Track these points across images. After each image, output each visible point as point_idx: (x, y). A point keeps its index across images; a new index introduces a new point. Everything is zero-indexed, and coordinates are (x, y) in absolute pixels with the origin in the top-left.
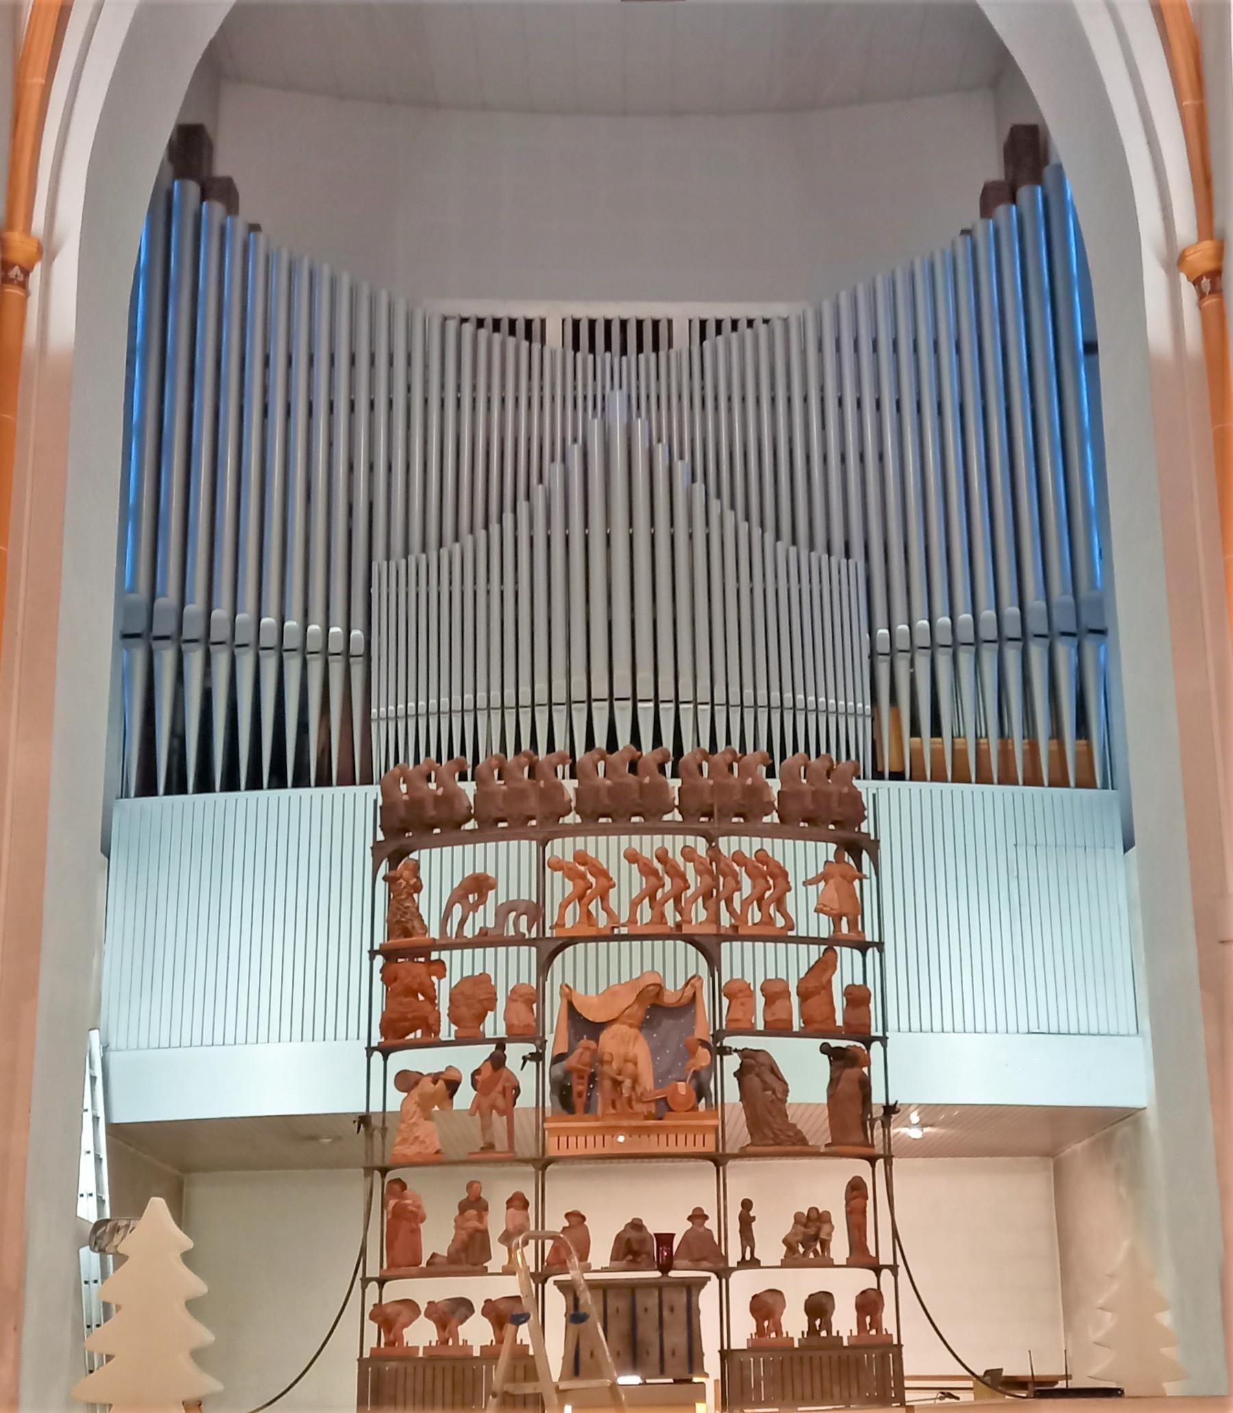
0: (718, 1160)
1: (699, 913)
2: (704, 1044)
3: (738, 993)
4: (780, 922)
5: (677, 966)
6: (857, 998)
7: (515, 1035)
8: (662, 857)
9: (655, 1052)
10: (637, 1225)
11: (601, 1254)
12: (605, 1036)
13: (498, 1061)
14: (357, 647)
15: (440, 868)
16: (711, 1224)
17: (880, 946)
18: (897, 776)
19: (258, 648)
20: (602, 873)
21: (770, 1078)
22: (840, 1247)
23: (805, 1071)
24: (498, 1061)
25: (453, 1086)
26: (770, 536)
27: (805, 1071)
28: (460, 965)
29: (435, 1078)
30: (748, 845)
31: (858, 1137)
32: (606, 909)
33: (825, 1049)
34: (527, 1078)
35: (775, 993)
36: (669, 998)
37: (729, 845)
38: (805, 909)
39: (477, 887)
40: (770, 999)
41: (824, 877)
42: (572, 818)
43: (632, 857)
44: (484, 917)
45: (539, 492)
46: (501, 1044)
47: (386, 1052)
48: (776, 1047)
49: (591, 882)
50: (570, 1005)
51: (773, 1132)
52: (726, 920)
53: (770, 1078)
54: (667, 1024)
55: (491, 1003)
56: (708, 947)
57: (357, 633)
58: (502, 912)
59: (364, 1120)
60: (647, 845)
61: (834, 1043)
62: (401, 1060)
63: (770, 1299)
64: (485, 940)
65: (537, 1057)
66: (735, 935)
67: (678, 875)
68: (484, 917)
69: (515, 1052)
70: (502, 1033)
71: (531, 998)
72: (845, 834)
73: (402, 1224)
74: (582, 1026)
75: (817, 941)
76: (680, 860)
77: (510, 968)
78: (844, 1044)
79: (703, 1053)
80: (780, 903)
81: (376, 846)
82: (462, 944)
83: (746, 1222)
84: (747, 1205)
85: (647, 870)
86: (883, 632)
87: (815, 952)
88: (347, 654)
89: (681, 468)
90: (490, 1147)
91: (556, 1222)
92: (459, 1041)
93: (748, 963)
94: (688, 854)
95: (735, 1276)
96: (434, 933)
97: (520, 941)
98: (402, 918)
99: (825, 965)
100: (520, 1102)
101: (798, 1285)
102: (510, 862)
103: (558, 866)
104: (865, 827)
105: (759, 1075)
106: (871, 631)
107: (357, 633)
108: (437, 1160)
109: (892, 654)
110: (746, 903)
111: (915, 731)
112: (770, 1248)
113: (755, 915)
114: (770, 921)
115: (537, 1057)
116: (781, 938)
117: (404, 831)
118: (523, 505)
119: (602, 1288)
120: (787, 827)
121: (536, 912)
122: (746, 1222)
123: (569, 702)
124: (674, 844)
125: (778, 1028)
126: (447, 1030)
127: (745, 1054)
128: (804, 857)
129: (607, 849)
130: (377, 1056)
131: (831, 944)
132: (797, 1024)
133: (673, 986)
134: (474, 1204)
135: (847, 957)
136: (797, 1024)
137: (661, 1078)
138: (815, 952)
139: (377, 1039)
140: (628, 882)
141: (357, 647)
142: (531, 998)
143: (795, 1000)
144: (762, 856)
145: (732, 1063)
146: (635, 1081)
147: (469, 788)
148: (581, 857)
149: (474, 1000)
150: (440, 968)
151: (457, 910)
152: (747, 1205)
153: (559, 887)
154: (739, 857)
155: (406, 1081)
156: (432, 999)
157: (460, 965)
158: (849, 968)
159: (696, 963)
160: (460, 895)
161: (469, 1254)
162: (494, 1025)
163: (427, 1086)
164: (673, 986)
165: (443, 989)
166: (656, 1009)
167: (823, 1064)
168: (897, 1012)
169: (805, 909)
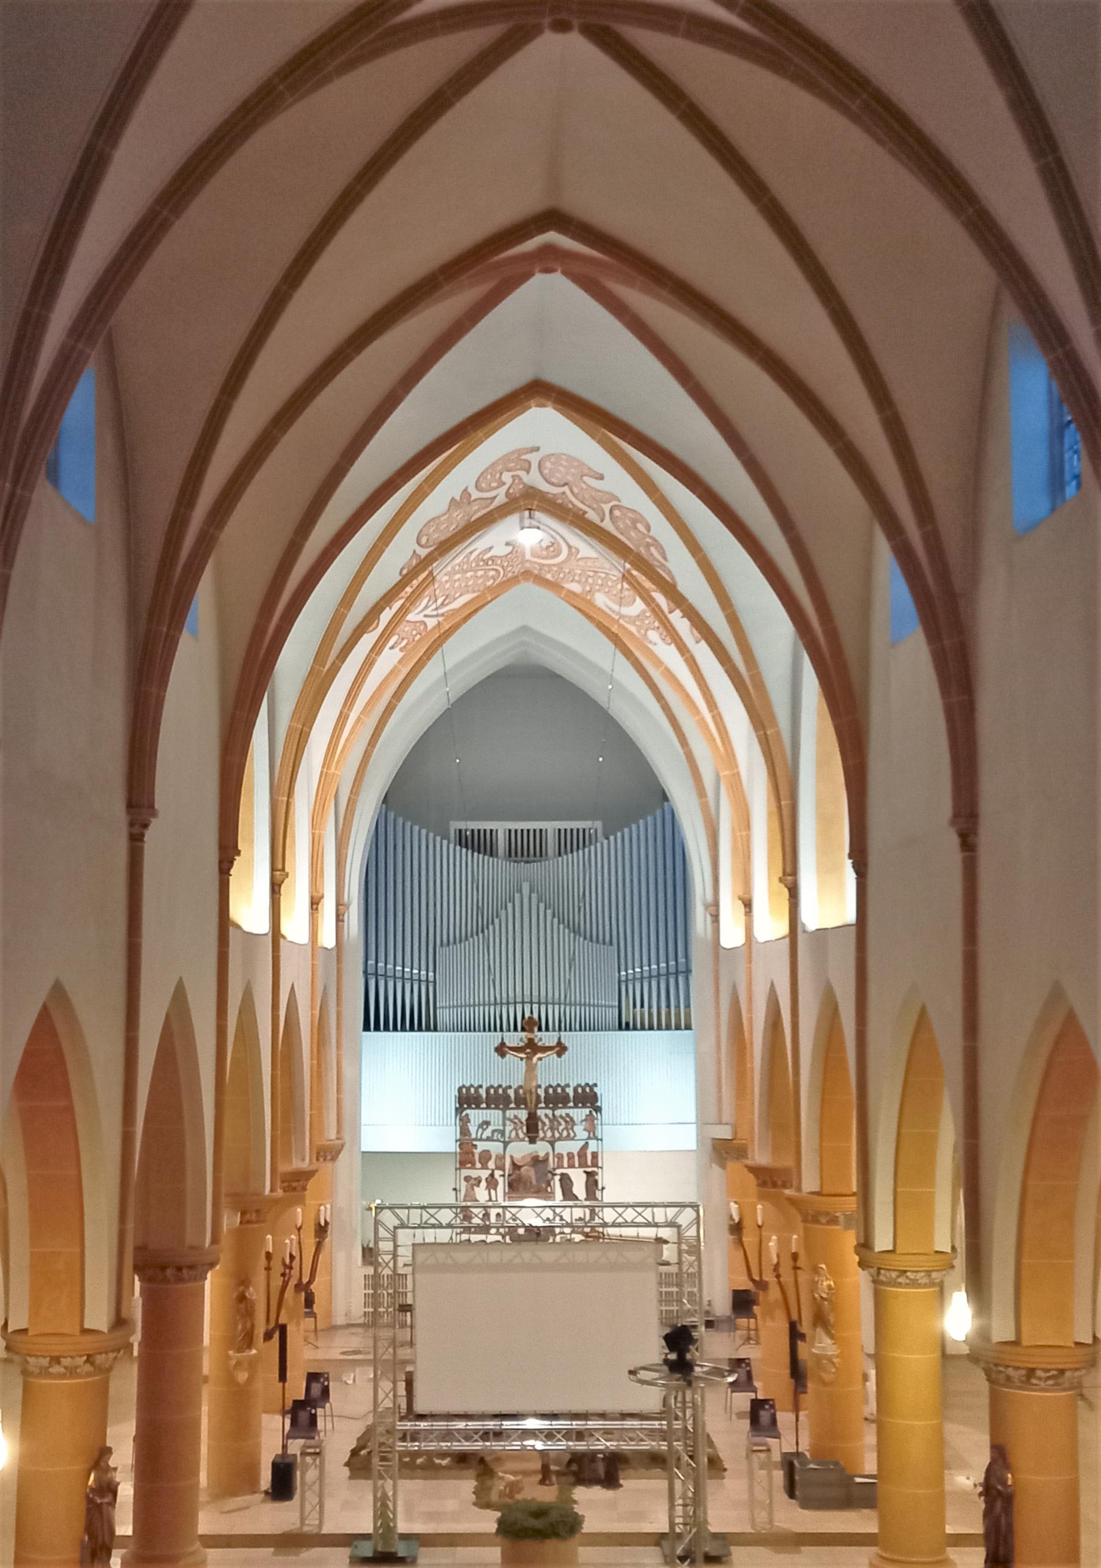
3: (560, 1157)
6: (595, 1155)
7: (497, 1168)
9: (536, 1173)
12: (522, 1169)
13: (492, 1175)
14: (431, 979)
19: (395, 977)
23: (578, 1178)
24: (492, 1175)
25: (480, 1182)
26: (582, 939)
27: (578, 1178)
28: (481, 1146)
34: (501, 1180)
35: (570, 1156)
37: (558, 1112)
40: (569, 1159)
42: (512, 1105)
44: (488, 1133)
45: (496, 921)
48: (571, 1172)
52: (557, 1135)
55: (490, 1158)
56: (552, 1143)
57: (431, 974)
58: (493, 1131)
62: (465, 1172)
64: (488, 1139)
65: (503, 1176)
66: (559, 1139)
68: (488, 1133)
69: (497, 1173)
70: (493, 1167)
71: (501, 1158)
74: (515, 1166)
76: (543, 1118)
77: (495, 1148)
79: (550, 1175)
80: (572, 1129)
81: (457, 1109)
82: (481, 1140)
88: (427, 981)
89: (549, 912)
92: (482, 1168)
93: (563, 1147)
94: (546, 1116)
96: (474, 1136)
97: (498, 1140)
98: (464, 1131)
99: (586, 1145)
102: (494, 1116)
103: (510, 1120)
104: (599, 1104)
105: (566, 1182)
106: (619, 972)
107: (431, 974)
109: (627, 981)
111: (635, 1006)
113: (565, 1133)
114: (569, 1134)
115: (503, 1176)
116: (573, 1139)
118: (491, 927)
120: (576, 1106)
121: (503, 1133)
126: (478, 1165)
128: (579, 1114)
132: (577, 1165)
133: (542, 1154)
136: (577, 1165)
141: (431, 979)
142: (501, 1158)
143: (576, 1158)
144: (568, 1115)
145: (557, 1178)
149: (485, 1156)
150: (475, 1146)
151: (480, 1131)
153: (509, 1127)
154: (561, 1117)
157: (481, 1146)
158: (593, 1146)
160: (480, 1126)
161: (485, 1229)
162: (491, 1164)
163: (472, 1182)
164: (542, 1154)
165: (477, 1152)
166: (537, 1162)
167: (585, 1175)
168: (605, 1161)
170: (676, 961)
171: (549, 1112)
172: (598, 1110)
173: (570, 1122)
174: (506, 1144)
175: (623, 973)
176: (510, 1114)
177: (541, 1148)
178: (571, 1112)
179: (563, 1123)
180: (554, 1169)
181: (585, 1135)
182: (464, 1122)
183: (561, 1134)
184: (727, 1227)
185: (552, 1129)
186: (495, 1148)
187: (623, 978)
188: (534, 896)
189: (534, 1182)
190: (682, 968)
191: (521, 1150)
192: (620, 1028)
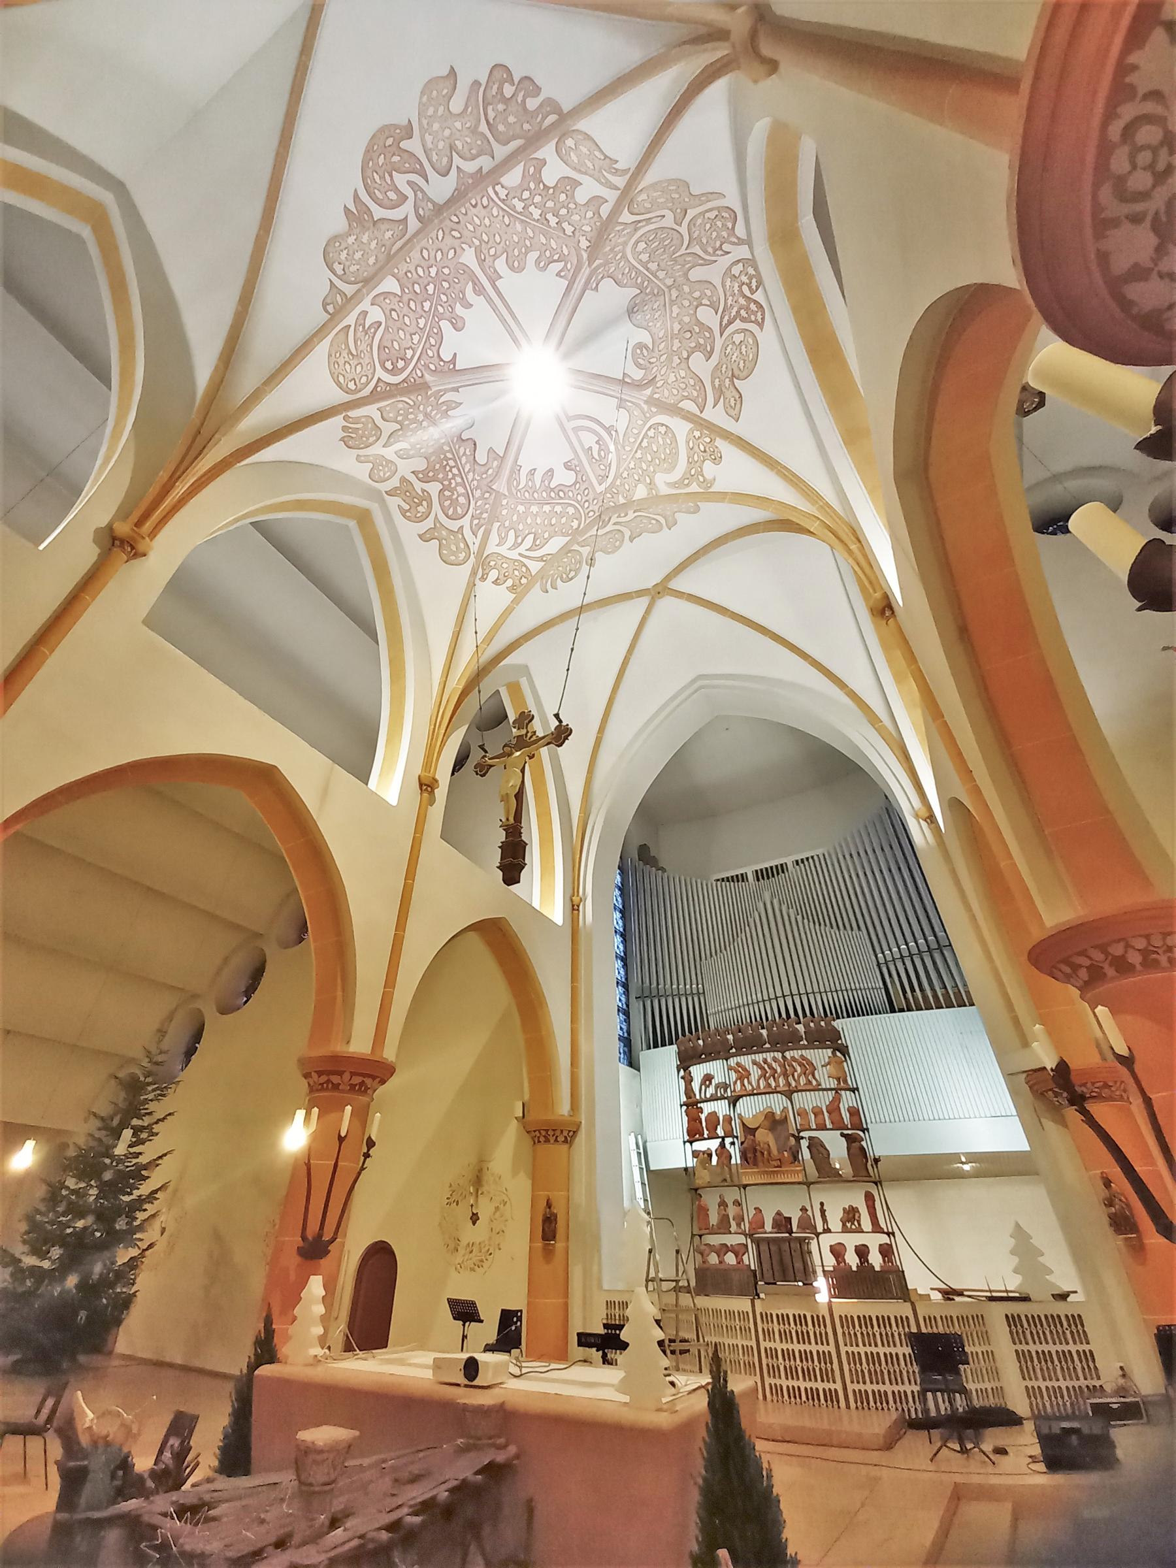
0: (808, 1184)
1: (782, 1081)
2: (793, 1135)
3: (802, 1113)
4: (814, 1083)
5: (777, 1103)
6: (854, 1112)
8: (765, 1061)
9: (777, 1140)
10: (779, 1213)
11: (768, 1227)
13: (722, 1145)
15: (698, 1072)
16: (809, 1212)
17: (857, 1089)
18: (901, 1010)
20: (745, 1069)
21: (822, 1149)
22: (866, 1224)
24: (722, 1145)
25: (710, 1155)
29: (704, 1152)
30: (796, 1054)
31: (865, 1173)
32: (749, 1083)
33: (842, 1135)
35: (817, 1112)
36: (778, 1118)
37: (787, 1054)
38: (824, 1077)
39: (708, 1079)
41: (829, 1063)
43: (754, 1063)
44: (711, 1091)
46: (723, 1139)
47: (691, 1143)
49: (743, 1074)
50: (744, 1124)
51: (826, 1173)
53: (822, 1149)
54: (779, 1128)
56: (789, 1094)
58: (717, 1087)
59: (686, 1169)
60: (759, 1058)
61: (846, 1132)
63: (837, 1248)
64: (714, 1098)
67: (770, 1067)
68: (711, 1091)
69: (728, 1141)
71: (728, 1120)
72: (835, 1046)
73: (703, 1211)
74: (749, 1131)
75: (831, 1089)
77: (721, 1108)
78: (849, 1132)
82: (707, 1101)
83: (823, 1212)
84: (822, 1204)
85: (762, 1068)
86: (880, 955)
87: (831, 1094)
90: (725, 1180)
91: (752, 1212)
94: (775, 1059)
95: (821, 1237)
98: (689, 1092)
99: (837, 1099)
100: (733, 1161)
101: (851, 1241)
102: (717, 1069)
105: (816, 1146)
108: (710, 1186)
110: (799, 1076)
112: (835, 1223)
113: (803, 1081)
114: (810, 1082)
115: (733, 1143)
116: (818, 1089)
117: (686, 1061)
119: (769, 1241)
122: (823, 1212)
123: (776, 998)
124: (769, 1056)
125: (822, 1127)
127: (810, 1138)
128: (820, 1056)
129: (746, 1060)
130: (688, 1144)
131: (836, 1090)
132: (829, 1126)
134: (723, 1204)
135: (846, 1096)
136: (829, 1126)
137: (780, 1151)
138: (831, 1094)
139: (687, 1138)
140: (755, 1073)
143: (826, 1114)
145: (804, 1144)
146: (769, 1153)
147: (701, 1042)
148: (738, 1064)
152: (822, 1204)
154: (793, 1058)
155: (695, 1154)
156: (701, 1122)
157: (708, 1108)
159: (785, 1101)
161: (724, 1226)
165: (703, 1117)
166: (774, 1122)
169: (824, 1077)
170: (935, 936)
171: (779, 1055)
172: (844, 1050)
173: (809, 1068)
174: (734, 1101)
175: (880, 955)
176: (733, 1062)
177: (777, 1103)
178: (808, 1054)
179: (799, 1069)
180: (799, 1131)
181: (833, 1084)
182: (688, 1080)
183: (797, 1081)
184: (1106, 1221)
185: (786, 1075)
186: (721, 1108)
187: (882, 961)
188: (784, 908)
189: (775, 1151)
190: (944, 942)
191: (749, 1108)
192: (893, 1011)
